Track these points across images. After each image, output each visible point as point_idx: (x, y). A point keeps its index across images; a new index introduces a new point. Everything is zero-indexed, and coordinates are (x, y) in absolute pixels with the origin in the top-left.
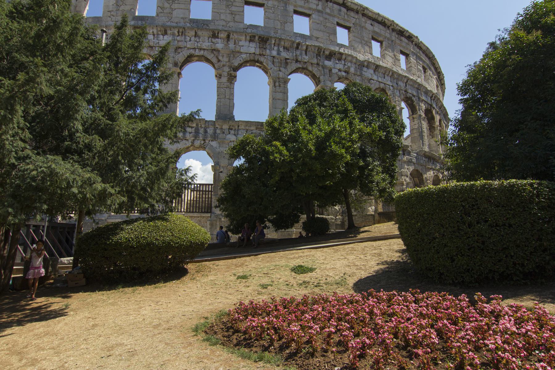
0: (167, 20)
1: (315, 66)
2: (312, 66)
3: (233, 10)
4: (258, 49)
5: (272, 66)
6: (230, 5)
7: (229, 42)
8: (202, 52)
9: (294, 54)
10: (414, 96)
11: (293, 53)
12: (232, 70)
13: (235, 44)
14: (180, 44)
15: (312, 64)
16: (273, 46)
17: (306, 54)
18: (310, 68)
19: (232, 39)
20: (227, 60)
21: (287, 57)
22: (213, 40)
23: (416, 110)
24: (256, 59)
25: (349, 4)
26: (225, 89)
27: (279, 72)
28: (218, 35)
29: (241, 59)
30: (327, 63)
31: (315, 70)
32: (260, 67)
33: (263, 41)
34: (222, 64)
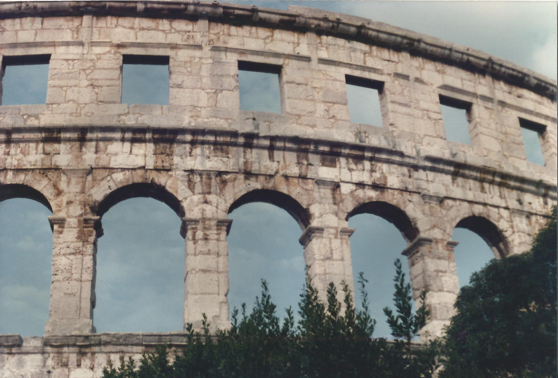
1: (296, 181)
2: (288, 185)
3: (96, 77)
5: (189, 192)
6: (89, 68)
7: (84, 149)
9: (242, 160)
11: (239, 157)
13: (96, 152)
16: (188, 146)
17: (271, 157)
18: (283, 189)
19: (91, 140)
20: (78, 189)
21: (223, 169)
22: (49, 148)
25: (374, 34)
26: (72, 257)
27: (205, 206)
29: (111, 184)
34: (64, 199)
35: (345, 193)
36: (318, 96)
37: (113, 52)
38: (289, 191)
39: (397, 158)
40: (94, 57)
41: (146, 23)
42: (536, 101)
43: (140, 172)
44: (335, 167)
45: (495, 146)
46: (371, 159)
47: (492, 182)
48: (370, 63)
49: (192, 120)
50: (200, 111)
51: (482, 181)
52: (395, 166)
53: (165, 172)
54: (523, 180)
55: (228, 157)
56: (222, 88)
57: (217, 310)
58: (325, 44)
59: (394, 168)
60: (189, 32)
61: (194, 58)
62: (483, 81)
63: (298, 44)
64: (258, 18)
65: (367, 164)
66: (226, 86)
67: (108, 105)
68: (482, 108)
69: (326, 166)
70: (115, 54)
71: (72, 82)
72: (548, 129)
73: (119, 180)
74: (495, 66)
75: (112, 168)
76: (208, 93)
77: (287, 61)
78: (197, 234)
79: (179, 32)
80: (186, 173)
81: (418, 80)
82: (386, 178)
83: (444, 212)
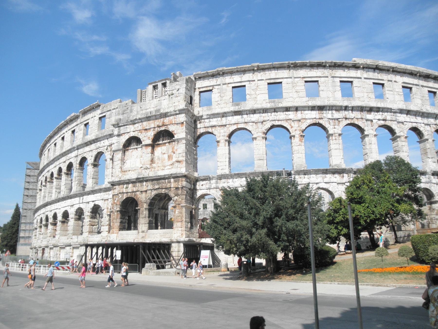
0: (254, 103)
1: (360, 120)
2: (358, 121)
8: (280, 122)
9: (344, 114)
14: (266, 119)
15: (357, 119)
17: (352, 112)
18: (356, 122)
22: (287, 113)
26: (298, 146)
28: (290, 110)
31: (360, 123)
33: (321, 108)
34: (294, 129)
36: (365, 90)
40: (296, 82)
43: (315, 119)
45: (419, 102)
48: (380, 78)
49: (328, 102)
66: (337, 90)
71: (290, 91)
77: (354, 79)
81: (395, 82)
82: (386, 117)
83: (404, 126)
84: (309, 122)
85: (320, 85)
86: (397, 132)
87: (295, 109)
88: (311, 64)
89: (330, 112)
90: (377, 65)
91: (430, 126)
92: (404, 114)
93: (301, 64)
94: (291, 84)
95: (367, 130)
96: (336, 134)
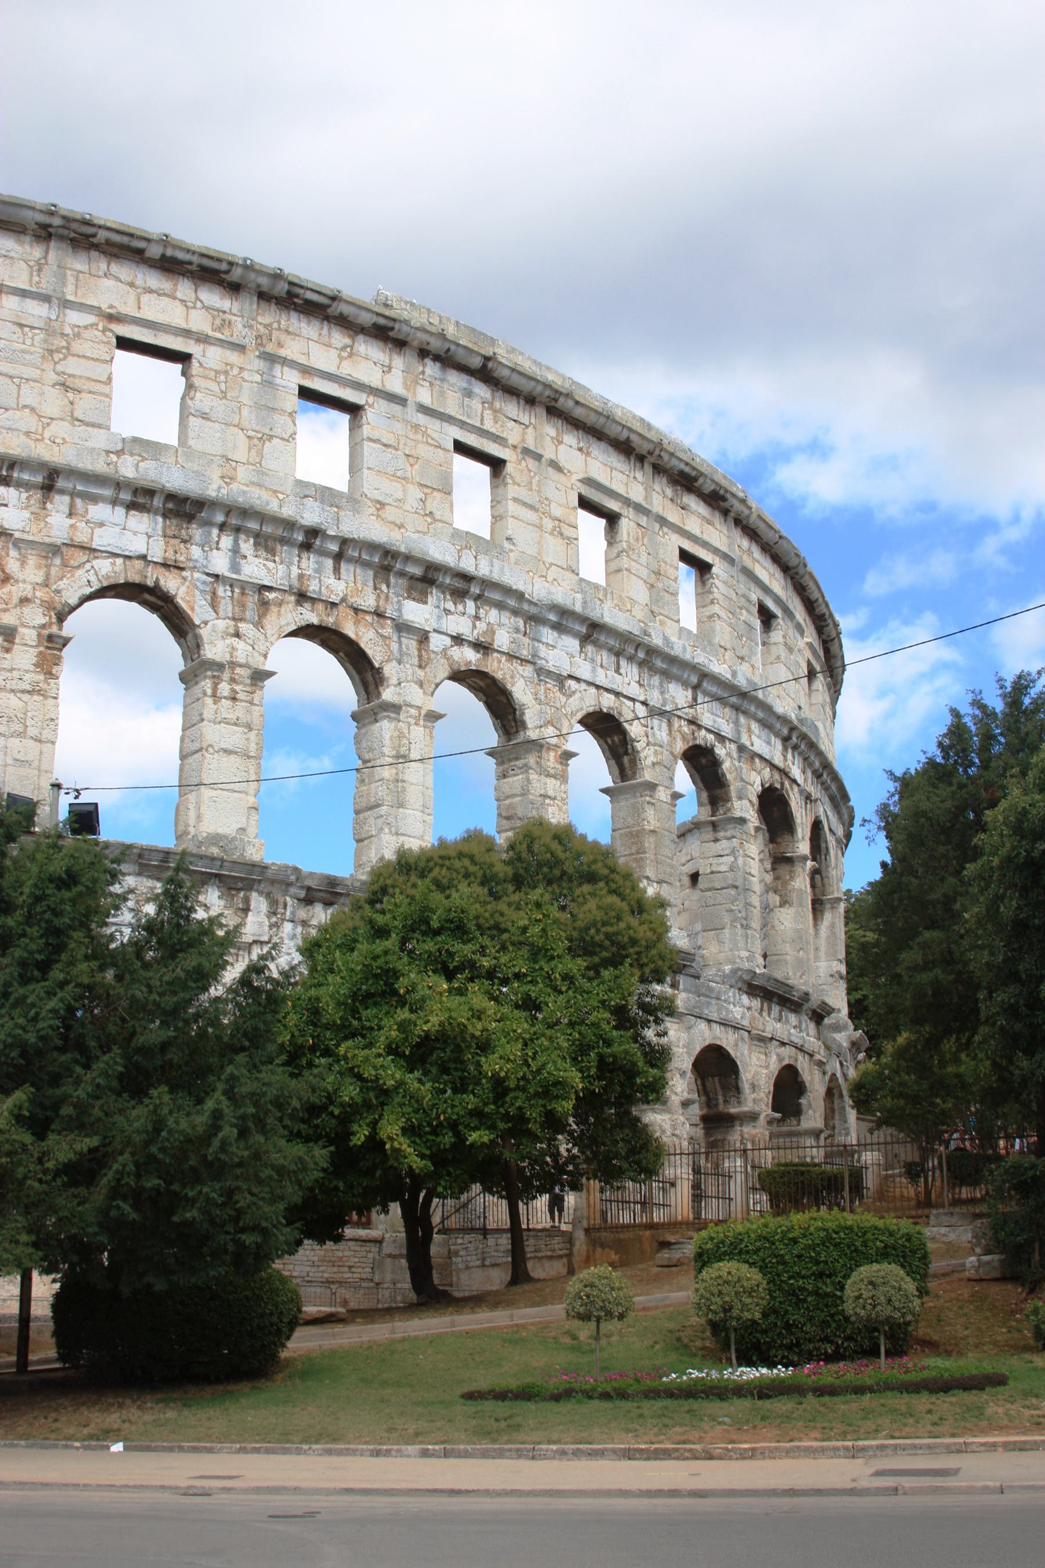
1: (369, 618)
2: (357, 623)
4: (161, 542)
5: (210, 614)
6: (58, 351)
7: (49, 506)
9: (295, 571)
10: (721, 738)
11: (291, 563)
12: (54, 620)
13: (70, 515)
15: (356, 610)
16: (215, 532)
17: (337, 570)
18: (349, 630)
19: (62, 492)
23: (728, 799)
24: (150, 583)
25: (506, 373)
26: (26, 697)
27: (235, 641)
29: (93, 578)
30: (416, 612)
32: (153, 608)
35: (435, 649)
36: (413, 472)
37: (100, 327)
38: (357, 635)
39: (512, 602)
40: (68, 330)
41: (154, 280)
42: (704, 518)
43: (139, 564)
44: (426, 603)
46: (477, 598)
47: (631, 659)
50: (235, 469)
51: (618, 654)
52: (508, 614)
53: (176, 571)
54: (673, 660)
55: (275, 561)
56: (271, 433)
57: (244, 820)
58: (430, 376)
59: (506, 618)
60: (224, 312)
61: (232, 366)
62: (639, 475)
63: (390, 368)
64: (338, 311)
65: (470, 605)
66: (278, 431)
67: (90, 429)
68: (632, 524)
69: (414, 599)
70: (104, 331)
72: (714, 570)
73: (103, 572)
74: (663, 454)
75: (95, 550)
76: (249, 437)
77: (371, 400)
78: (220, 686)
79: (207, 308)
80: (210, 579)
82: (494, 633)
83: (563, 699)
84: (106, 570)
85: (197, 381)
86: (530, 724)
87: (39, 479)
88: (169, 252)
89: (227, 541)
90: (487, 359)
91: (670, 724)
92: (575, 634)
93: (116, 238)
94: (40, 336)
95: (394, 681)
96: (238, 670)
